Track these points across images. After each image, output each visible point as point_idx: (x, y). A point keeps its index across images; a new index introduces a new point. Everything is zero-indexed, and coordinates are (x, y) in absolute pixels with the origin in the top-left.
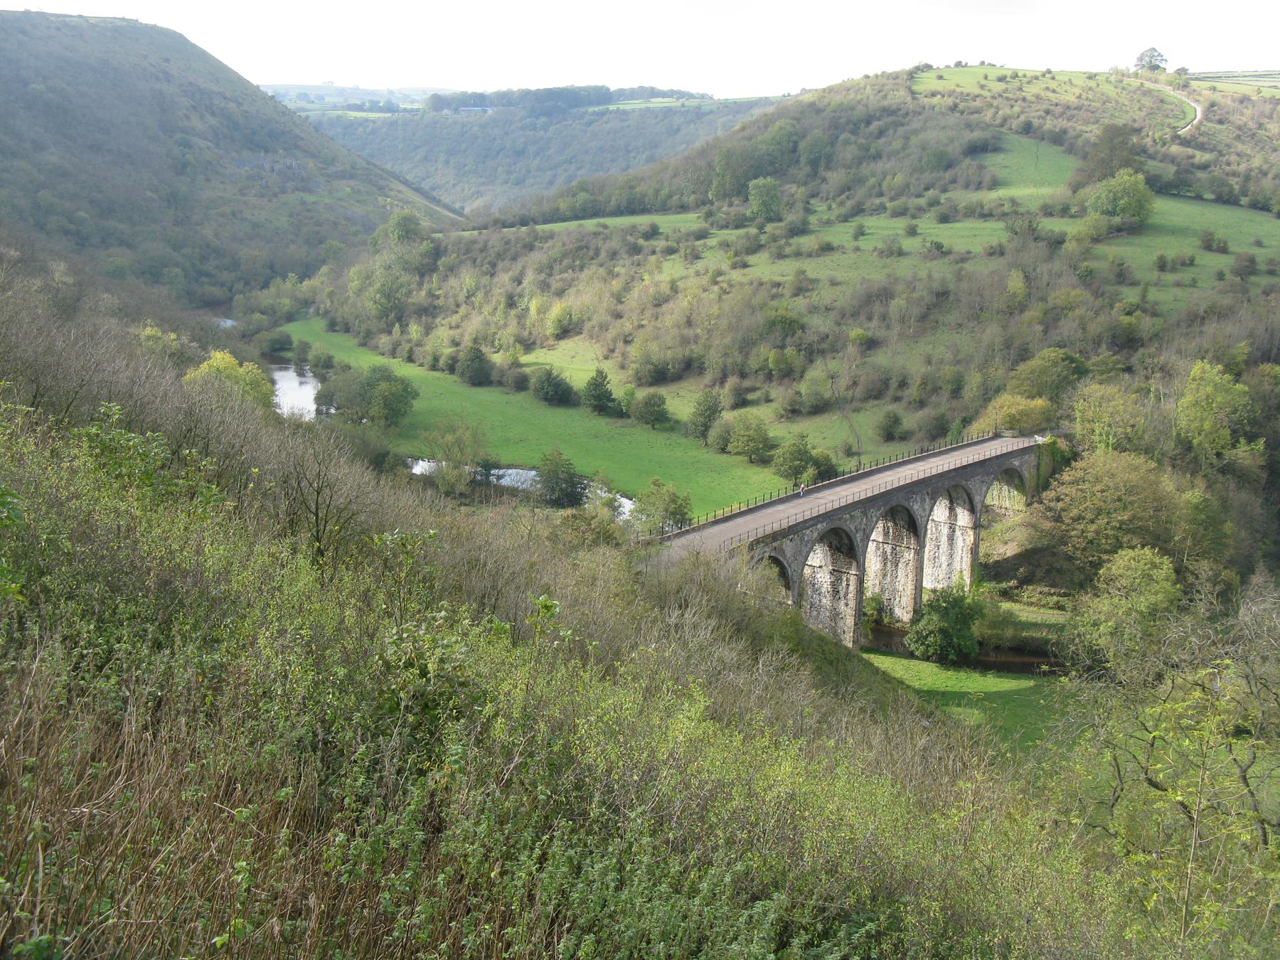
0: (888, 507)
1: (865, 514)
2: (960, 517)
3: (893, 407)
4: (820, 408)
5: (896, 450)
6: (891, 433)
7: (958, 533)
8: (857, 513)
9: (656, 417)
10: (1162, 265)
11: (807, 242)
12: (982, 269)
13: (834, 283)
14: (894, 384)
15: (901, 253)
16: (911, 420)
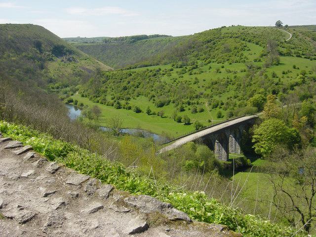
3: (221, 110)
5: (221, 120)
6: (220, 116)
13: (204, 80)
14: (220, 104)
16: (224, 113)
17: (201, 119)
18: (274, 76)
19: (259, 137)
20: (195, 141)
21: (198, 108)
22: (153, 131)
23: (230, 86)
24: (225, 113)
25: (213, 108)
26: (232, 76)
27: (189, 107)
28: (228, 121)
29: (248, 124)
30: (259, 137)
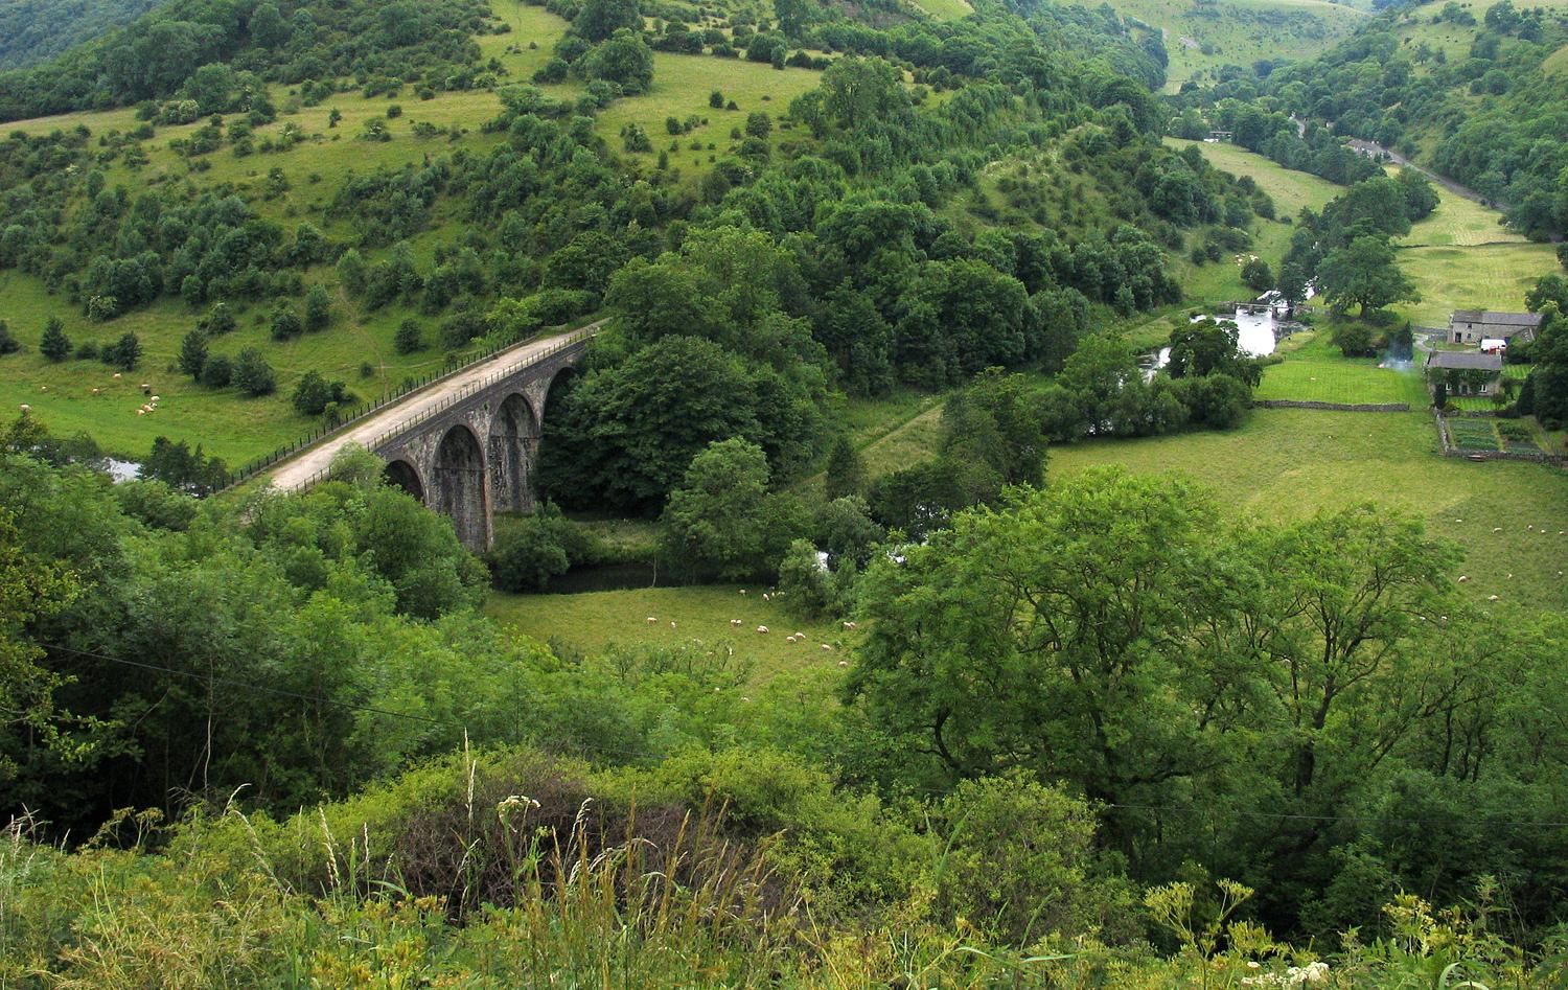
0: (447, 429)
2: (519, 428)
3: (410, 315)
4: (319, 321)
5: (417, 366)
6: (409, 344)
7: (521, 446)
8: (417, 440)
9: (125, 356)
10: (673, 128)
11: (272, 132)
12: (481, 151)
13: (315, 179)
15: (387, 138)
18: (638, 143)
19: (621, 429)
20: (345, 472)
21: (297, 309)
22: (102, 442)
23: (442, 203)
24: (431, 328)
25: (372, 309)
26: (442, 153)
27: (257, 310)
29: (562, 377)
30: (621, 429)
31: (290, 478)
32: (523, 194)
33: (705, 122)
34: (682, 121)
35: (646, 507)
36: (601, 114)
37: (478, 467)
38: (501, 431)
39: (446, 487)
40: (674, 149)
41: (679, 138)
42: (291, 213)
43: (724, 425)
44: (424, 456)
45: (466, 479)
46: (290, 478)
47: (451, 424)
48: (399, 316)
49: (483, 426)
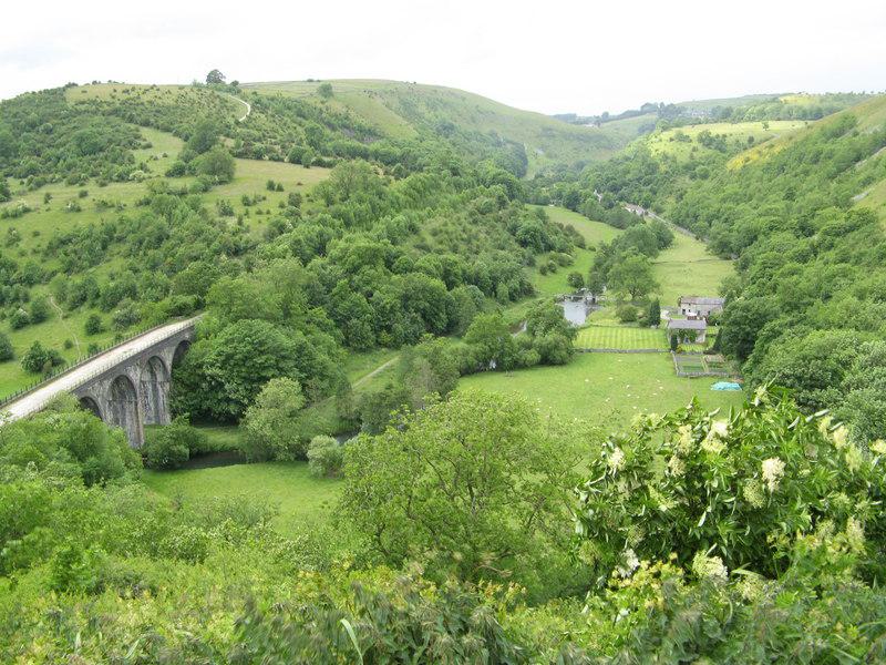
1: (101, 384)
3: (96, 312)
4: (40, 317)
5: (101, 340)
6: (94, 329)
7: (159, 386)
10: (246, 202)
12: (132, 214)
13: (36, 234)
15: (79, 210)
16: (106, 319)
17: (49, 337)
18: (227, 212)
20: (54, 406)
21: (24, 311)
23: (113, 248)
24: (106, 319)
25: (71, 309)
26: (110, 216)
28: (119, 340)
29: (182, 345)
31: (21, 409)
32: (160, 240)
33: (264, 199)
34: (251, 198)
35: (231, 421)
36: (206, 196)
37: (133, 399)
38: (147, 377)
39: (115, 412)
40: (247, 214)
41: (250, 209)
42: (22, 254)
43: (277, 371)
44: (101, 393)
45: (127, 406)
46: (21, 409)
47: (118, 375)
48: (85, 314)
49: (136, 375)
